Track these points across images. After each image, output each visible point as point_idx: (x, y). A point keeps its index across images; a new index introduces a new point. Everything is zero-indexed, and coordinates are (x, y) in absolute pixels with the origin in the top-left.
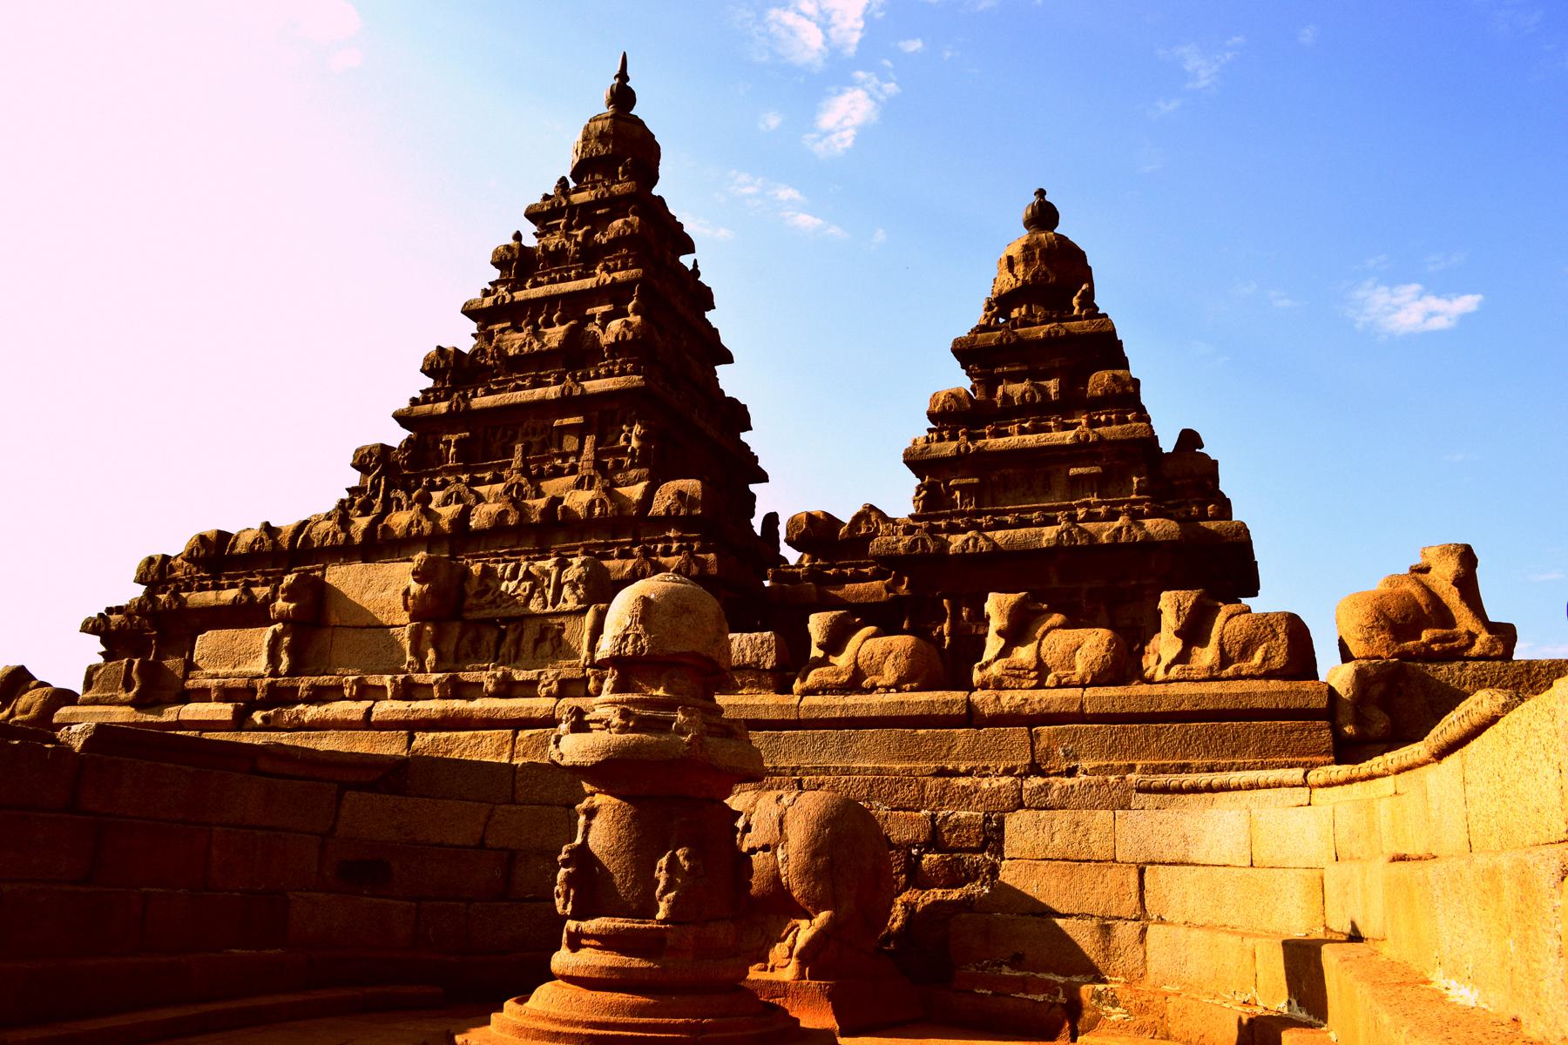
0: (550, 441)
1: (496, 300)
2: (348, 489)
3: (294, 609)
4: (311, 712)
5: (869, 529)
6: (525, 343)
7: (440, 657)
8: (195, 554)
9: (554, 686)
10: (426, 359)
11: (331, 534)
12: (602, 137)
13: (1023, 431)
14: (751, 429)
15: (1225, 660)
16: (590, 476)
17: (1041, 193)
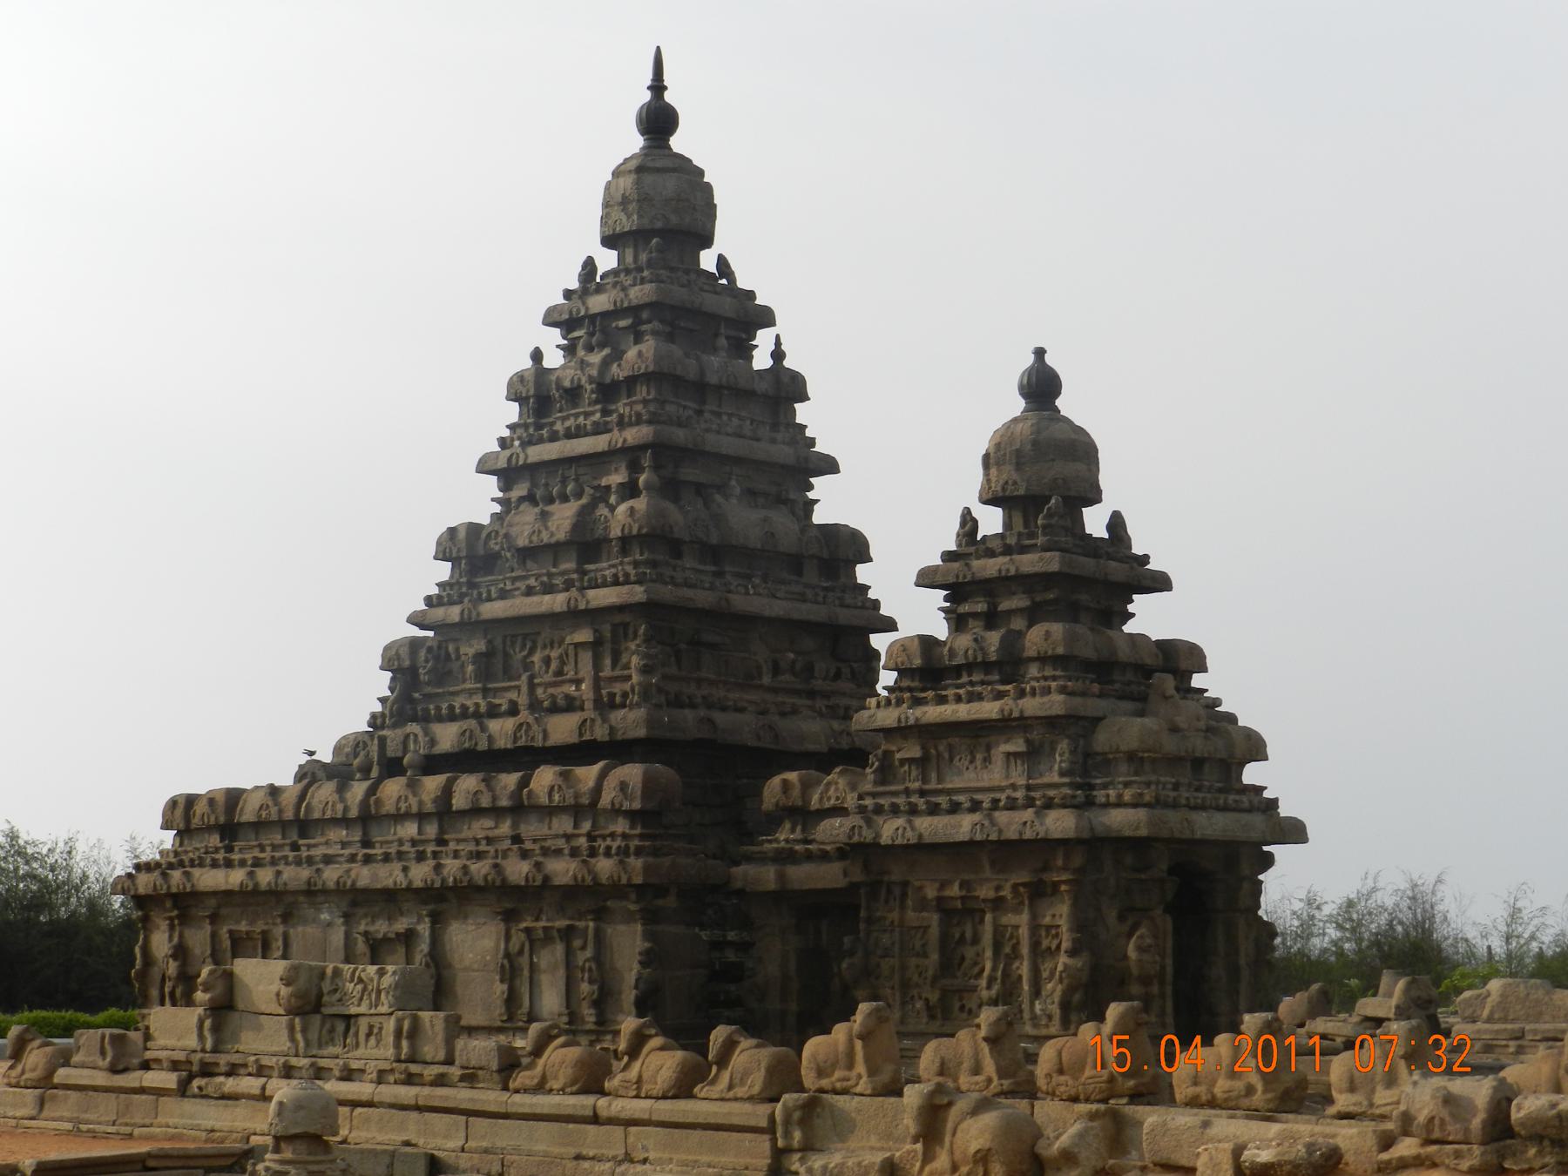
0: (567, 655)
1: (512, 455)
2: (383, 700)
3: (211, 1000)
4: (230, 1085)
5: (838, 799)
6: (534, 532)
7: (308, 1044)
8: (206, 820)
9: (374, 1076)
10: (439, 543)
11: (330, 804)
12: (624, 202)
13: (958, 699)
14: (870, 560)
15: (731, 1087)
16: (593, 720)
17: (1040, 353)
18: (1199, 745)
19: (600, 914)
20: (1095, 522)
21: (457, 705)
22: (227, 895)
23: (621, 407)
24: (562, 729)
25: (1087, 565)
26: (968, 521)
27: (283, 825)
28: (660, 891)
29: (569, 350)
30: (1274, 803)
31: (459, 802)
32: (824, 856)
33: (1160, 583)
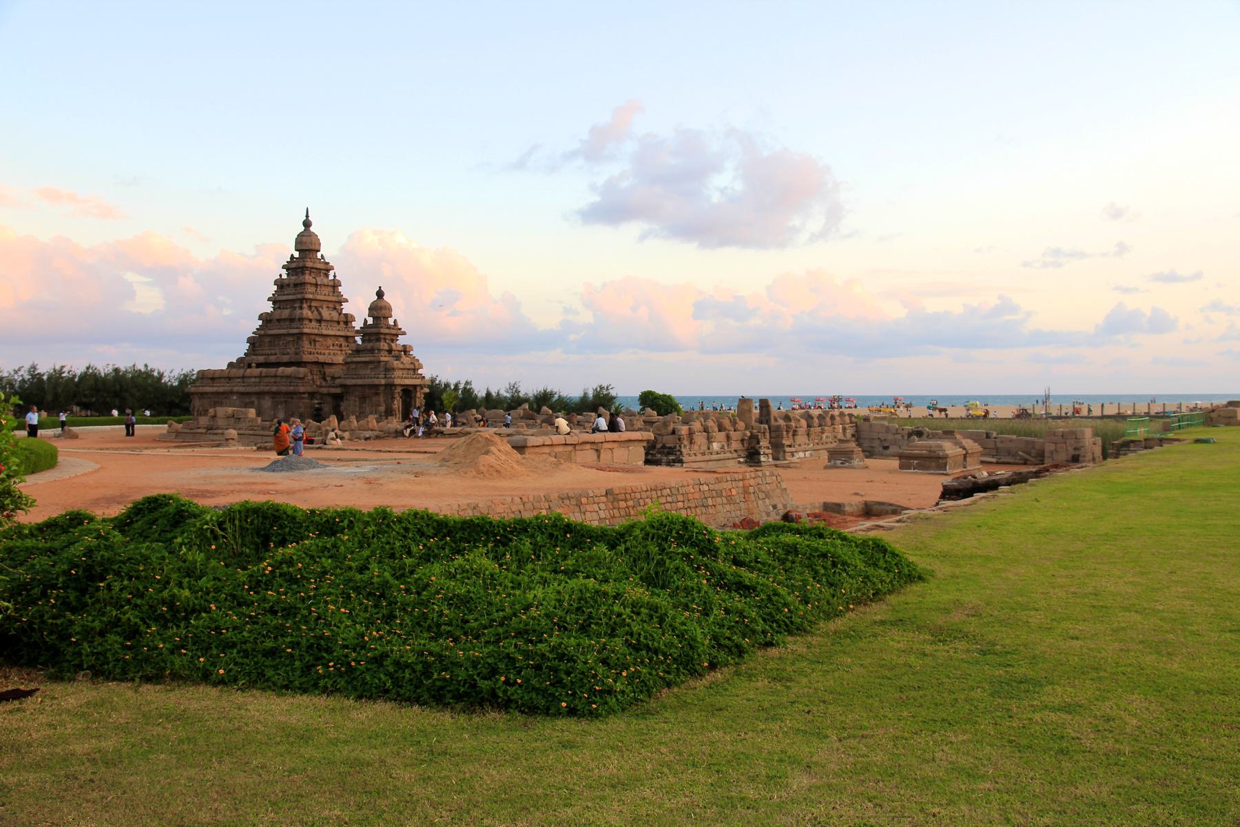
4: (216, 431)
18: (408, 367)
19: (292, 398)
20: (391, 321)
21: (264, 352)
22: (213, 393)
23: (298, 288)
24: (286, 359)
25: (387, 331)
26: (365, 320)
27: (225, 378)
28: (304, 393)
29: (288, 275)
30: (424, 377)
31: (263, 375)
32: (337, 387)
33: (404, 333)
